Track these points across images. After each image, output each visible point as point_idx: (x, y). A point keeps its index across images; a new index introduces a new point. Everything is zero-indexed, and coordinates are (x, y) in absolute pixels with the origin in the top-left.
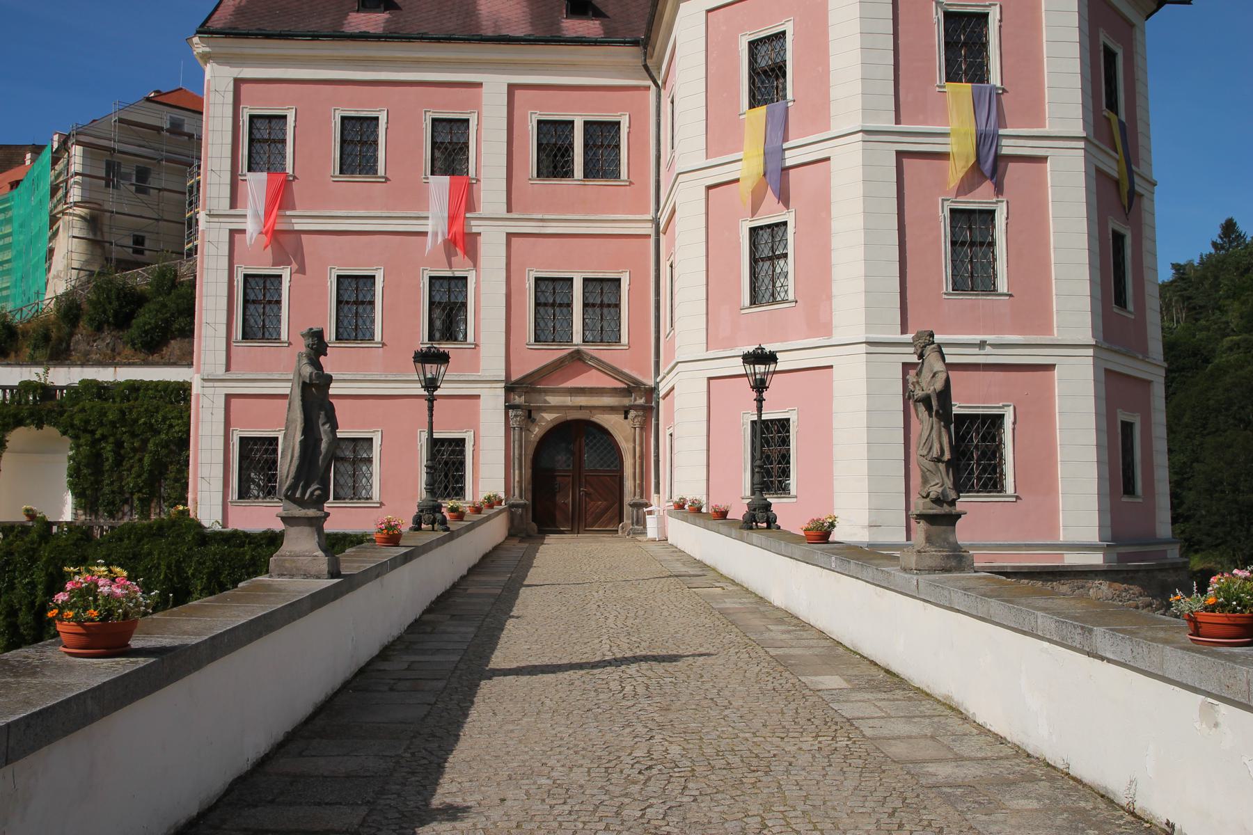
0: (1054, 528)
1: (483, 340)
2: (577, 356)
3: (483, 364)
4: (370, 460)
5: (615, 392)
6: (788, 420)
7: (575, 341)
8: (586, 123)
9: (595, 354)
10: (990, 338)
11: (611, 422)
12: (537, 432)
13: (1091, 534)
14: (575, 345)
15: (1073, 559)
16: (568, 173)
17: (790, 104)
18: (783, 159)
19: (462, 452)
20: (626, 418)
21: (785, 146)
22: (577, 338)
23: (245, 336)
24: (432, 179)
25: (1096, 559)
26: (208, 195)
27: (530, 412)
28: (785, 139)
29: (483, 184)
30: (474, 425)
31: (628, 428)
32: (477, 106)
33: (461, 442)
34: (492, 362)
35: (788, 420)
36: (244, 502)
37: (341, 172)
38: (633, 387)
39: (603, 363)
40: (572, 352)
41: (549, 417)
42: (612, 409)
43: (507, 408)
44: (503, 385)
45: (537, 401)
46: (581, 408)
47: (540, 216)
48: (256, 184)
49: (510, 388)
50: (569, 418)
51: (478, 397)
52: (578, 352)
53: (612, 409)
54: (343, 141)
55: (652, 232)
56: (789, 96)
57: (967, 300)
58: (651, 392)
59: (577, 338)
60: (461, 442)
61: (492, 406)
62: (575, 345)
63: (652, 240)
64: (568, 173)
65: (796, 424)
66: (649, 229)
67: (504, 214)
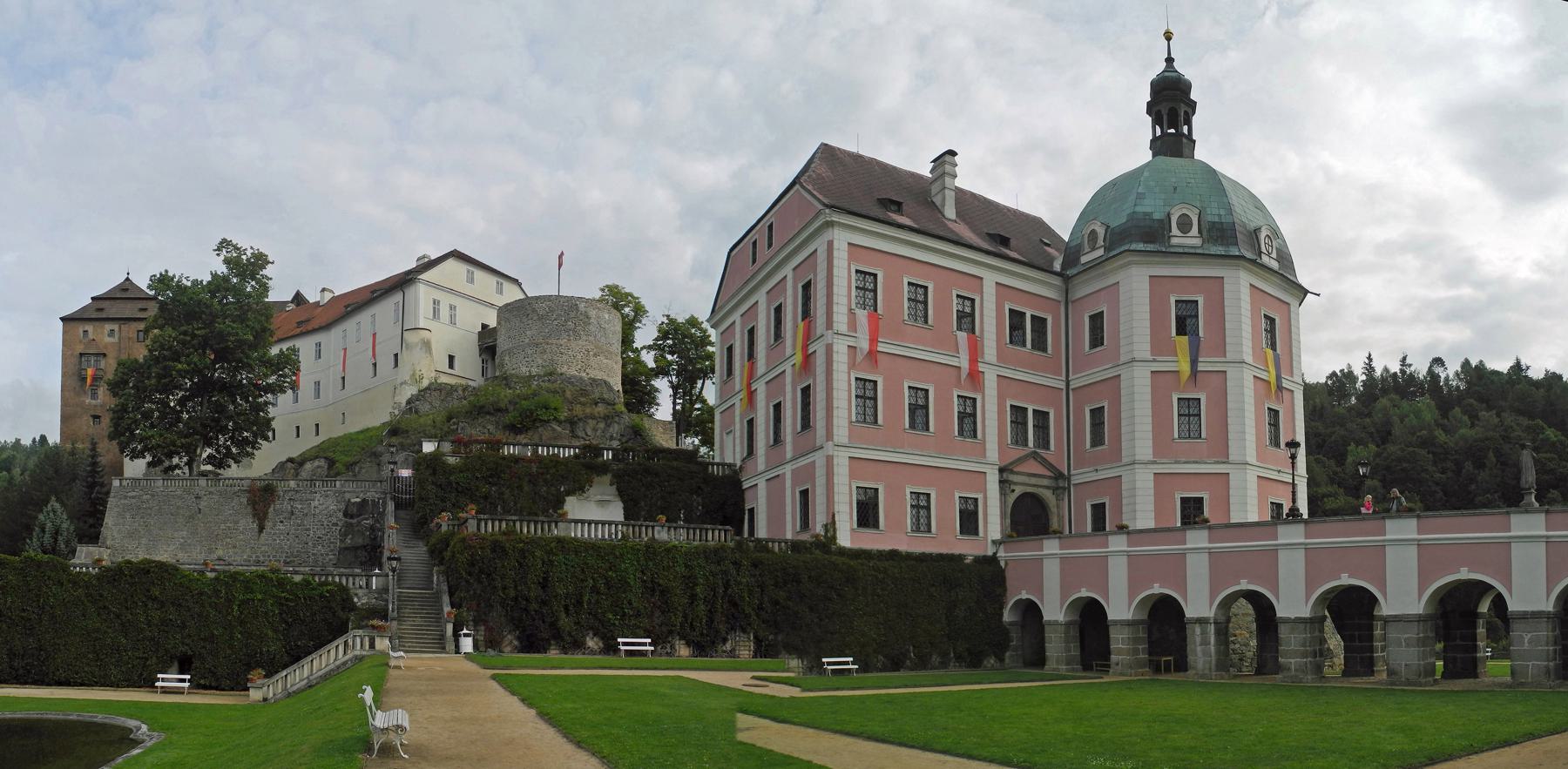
3: (988, 454)
5: (1050, 477)
9: (1043, 455)
11: (1048, 495)
12: (1012, 498)
22: (1031, 444)
34: (993, 453)
36: (862, 530)
38: (1059, 476)
41: (1019, 490)
42: (1047, 487)
43: (1000, 482)
44: (997, 467)
46: (1034, 486)
49: (1001, 471)
53: (1047, 487)
55: (1064, 387)
58: (1069, 479)
59: (1031, 444)
63: (1064, 392)
66: (1062, 385)
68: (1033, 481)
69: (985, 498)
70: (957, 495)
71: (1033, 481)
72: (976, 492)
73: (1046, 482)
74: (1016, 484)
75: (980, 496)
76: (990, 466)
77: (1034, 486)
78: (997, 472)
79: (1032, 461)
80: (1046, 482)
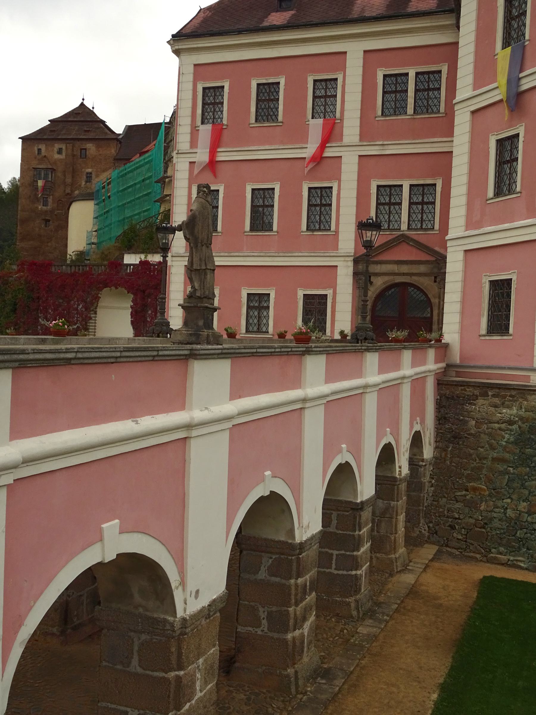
3: (340, 245)
4: (268, 307)
6: (511, 279)
7: (402, 229)
9: (415, 238)
14: (402, 231)
17: (527, 43)
18: (518, 86)
19: (325, 304)
20: (435, 281)
21: (521, 75)
24: (312, 122)
26: (177, 141)
27: (370, 277)
28: (521, 71)
29: (346, 123)
30: (334, 286)
31: (436, 288)
35: (511, 279)
37: (256, 121)
39: (420, 243)
40: (398, 236)
44: (352, 258)
45: (374, 268)
46: (404, 274)
47: (381, 143)
48: (205, 131)
50: (396, 281)
51: (337, 266)
52: (403, 235)
56: (527, 37)
59: (404, 227)
62: (402, 231)
65: (515, 282)
68: (405, 269)
69: (335, 293)
70: (301, 293)
71: (405, 269)
72: (324, 288)
73: (422, 269)
74: (377, 275)
75: (329, 292)
76: (342, 259)
78: (351, 264)
79: (404, 247)
80: (422, 269)
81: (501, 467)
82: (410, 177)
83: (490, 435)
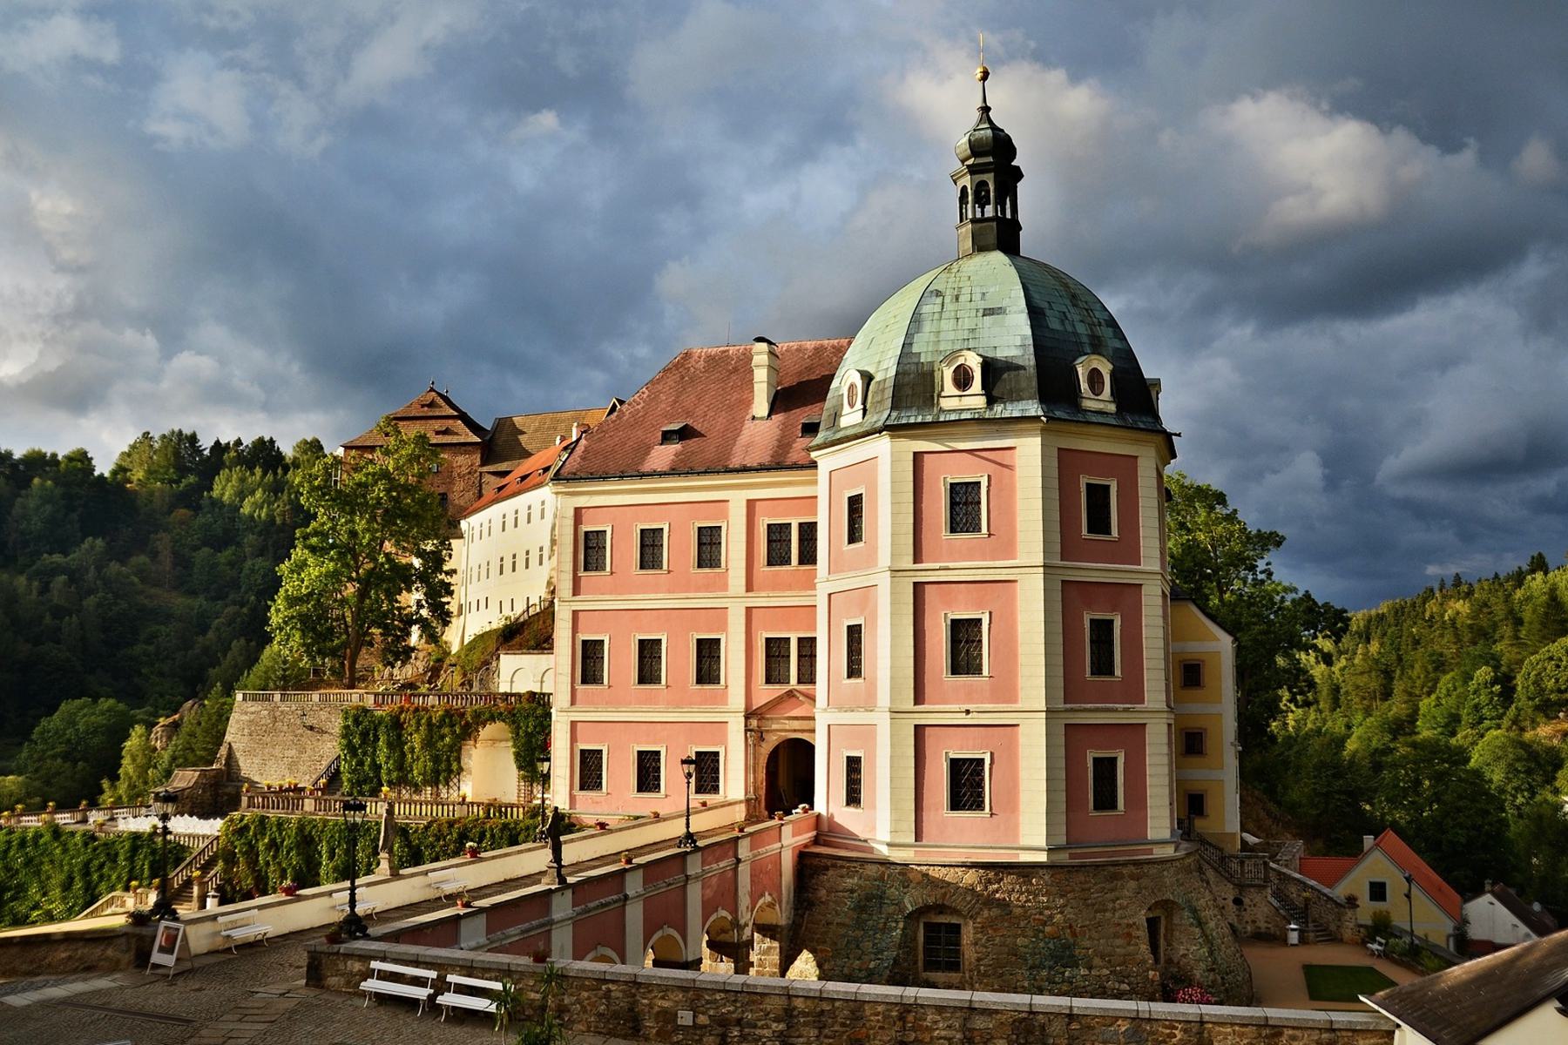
0: (1016, 836)
1: (729, 684)
2: (790, 694)
8: (801, 525)
10: (970, 707)
13: (1042, 841)
15: (1026, 857)
16: (788, 562)
23: (584, 681)
25: (1042, 857)
30: (724, 742)
32: (725, 516)
33: (717, 754)
34: (737, 699)
41: (772, 741)
43: (746, 731)
54: (642, 546)
57: (962, 679)
60: (717, 754)
61: (736, 726)
64: (788, 562)
67: (744, 594)
77: (795, 731)
81: (843, 931)
82: (797, 630)
83: (835, 902)
